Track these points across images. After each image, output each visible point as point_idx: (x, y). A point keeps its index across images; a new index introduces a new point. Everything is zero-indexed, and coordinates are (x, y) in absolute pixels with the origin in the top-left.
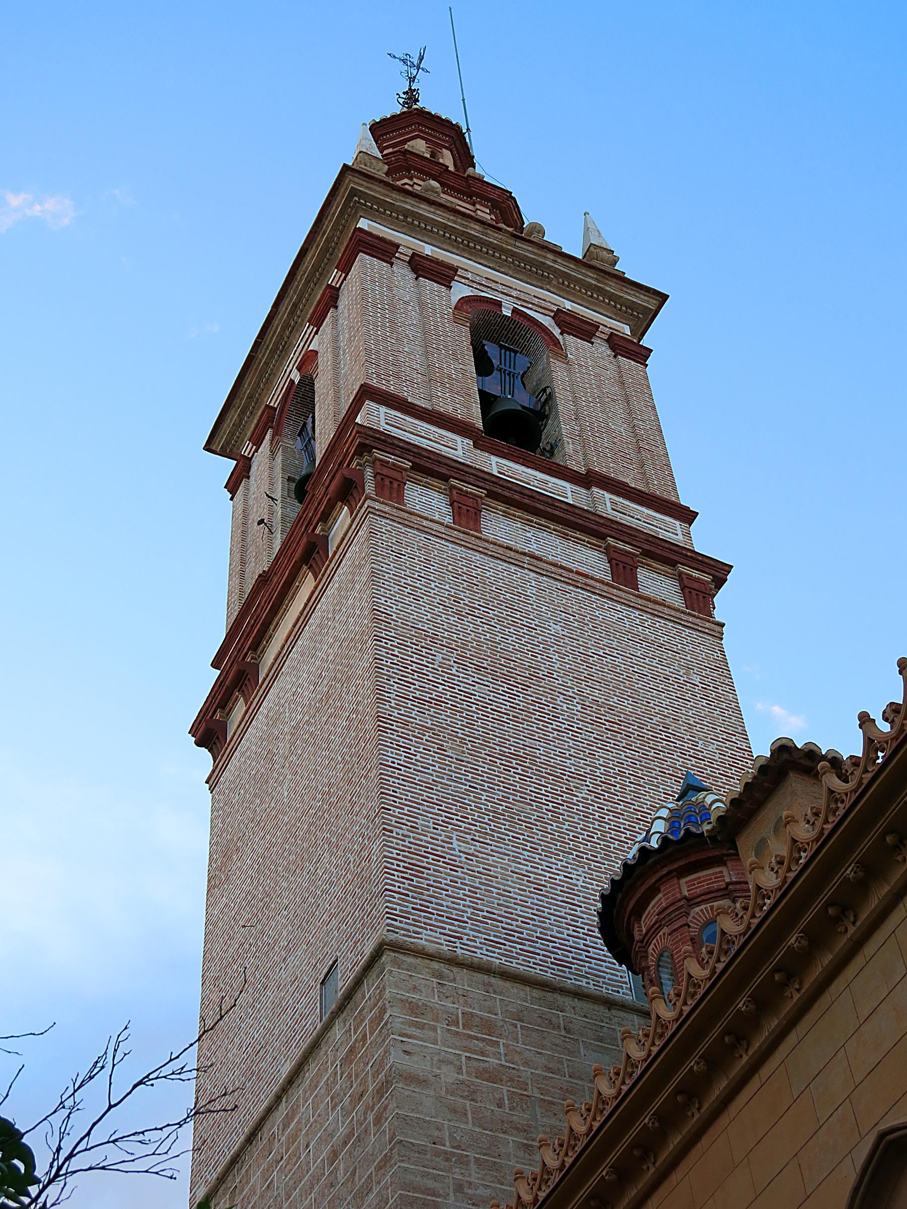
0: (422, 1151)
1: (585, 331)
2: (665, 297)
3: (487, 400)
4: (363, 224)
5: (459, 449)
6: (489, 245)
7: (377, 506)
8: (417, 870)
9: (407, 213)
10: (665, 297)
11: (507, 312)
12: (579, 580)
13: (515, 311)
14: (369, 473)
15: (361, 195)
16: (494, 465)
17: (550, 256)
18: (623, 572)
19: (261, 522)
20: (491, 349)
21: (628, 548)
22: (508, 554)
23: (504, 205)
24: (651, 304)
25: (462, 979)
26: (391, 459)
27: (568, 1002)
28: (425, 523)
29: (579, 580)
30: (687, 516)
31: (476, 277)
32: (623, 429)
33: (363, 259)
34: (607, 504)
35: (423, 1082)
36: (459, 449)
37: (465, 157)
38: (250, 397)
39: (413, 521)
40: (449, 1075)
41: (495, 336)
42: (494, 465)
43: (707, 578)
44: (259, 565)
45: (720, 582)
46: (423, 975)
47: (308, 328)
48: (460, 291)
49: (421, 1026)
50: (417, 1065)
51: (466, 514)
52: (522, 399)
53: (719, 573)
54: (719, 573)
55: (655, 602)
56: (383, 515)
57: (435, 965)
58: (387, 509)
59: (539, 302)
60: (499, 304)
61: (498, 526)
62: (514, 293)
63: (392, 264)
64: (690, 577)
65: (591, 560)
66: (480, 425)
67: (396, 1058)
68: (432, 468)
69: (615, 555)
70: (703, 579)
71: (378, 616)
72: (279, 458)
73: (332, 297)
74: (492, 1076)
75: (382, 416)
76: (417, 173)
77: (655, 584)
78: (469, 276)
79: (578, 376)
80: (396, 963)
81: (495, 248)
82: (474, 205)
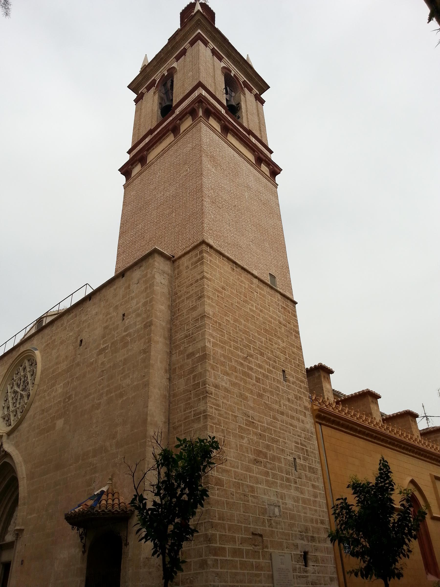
1: (250, 90)
3: (227, 100)
15: (201, 22)
29: (248, 161)
30: (271, 152)
31: (226, 63)
41: (230, 83)
52: (233, 103)
70: (275, 171)
73: (184, 52)
77: (264, 168)
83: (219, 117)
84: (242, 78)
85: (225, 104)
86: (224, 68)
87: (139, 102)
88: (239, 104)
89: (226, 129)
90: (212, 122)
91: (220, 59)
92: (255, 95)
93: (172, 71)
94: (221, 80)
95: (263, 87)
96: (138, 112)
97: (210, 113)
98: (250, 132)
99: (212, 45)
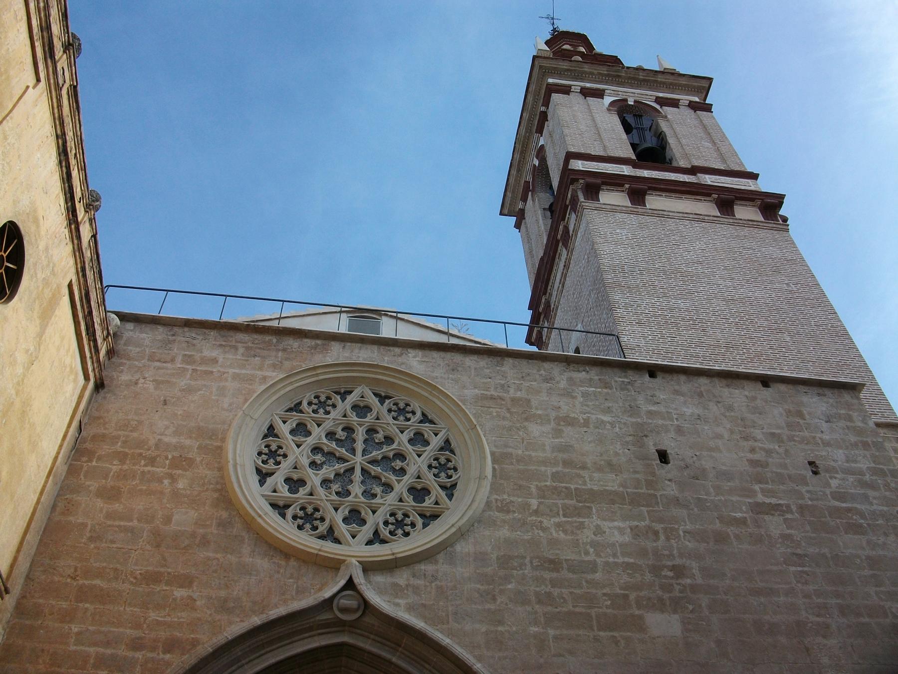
1: (674, 104)
2: (710, 80)
3: (634, 146)
4: (550, 81)
5: (626, 170)
16: (646, 173)
23: (615, 61)
24: (705, 84)
34: (708, 179)
36: (626, 170)
37: (590, 46)
42: (646, 173)
47: (536, 135)
52: (650, 142)
59: (648, 96)
61: (654, 201)
65: (707, 208)
66: (634, 157)
76: (568, 59)
77: (743, 212)
83: (614, 182)
84: (648, 96)
85: (630, 154)
86: (612, 103)
87: (523, 227)
88: (661, 138)
89: (638, 193)
90: (608, 197)
91: (599, 94)
92: (689, 106)
94: (614, 121)
95: (702, 84)
96: (527, 240)
97: (594, 185)
98: (693, 170)
99: (577, 85)
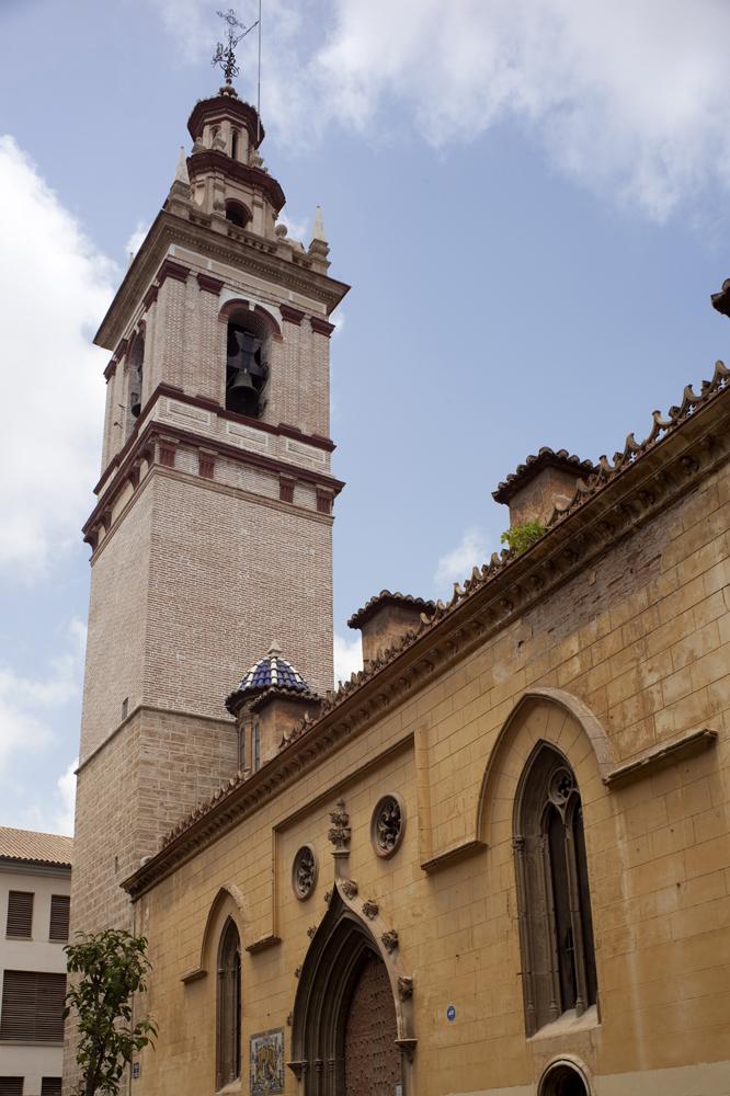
0: (148, 791)
2: (348, 288)
6: (247, 259)
7: (159, 469)
8: (159, 671)
9: (198, 240)
10: (348, 288)
11: (252, 308)
12: (261, 500)
13: (257, 307)
14: (157, 447)
17: (282, 264)
18: (287, 492)
19: (116, 424)
20: (238, 334)
21: (291, 477)
22: (226, 490)
25: (173, 720)
26: (169, 439)
27: (217, 726)
28: (184, 476)
29: (261, 500)
32: (305, 387)
33: (169, 280)
35: (151, 764)
38: (116, 322)
39: (179, 476)
40: (162, 760)
43: (331, 490)
44: (116, 450)
45: (338, 492)
46: (157, 720)
48: (228, 295)
49: (153, 741)
50: (148, 757)
51: (207, 467)
53: (338, 486)
54: (338, 486)
55: (300, 508)
56: (161, 474)
57: (162, 714)
58: (163, 470)
60: (247, 303)
61: (225, 473)
62: (258, 293)
63: (185, 283)
64: (322, 490)
65: (269, 487)
67: (142, 756)
68: (190, 441)
69: (285, 483)
71: (155, 538)
72: (127, 379)
74: (181, 759)
75: (168, 406)
77: (305, 498)
78: (232, 283)
79: (286, 352)
80: (145, 715)
81: (250, 261)
82: (253, 189)
93: (142, 324)
